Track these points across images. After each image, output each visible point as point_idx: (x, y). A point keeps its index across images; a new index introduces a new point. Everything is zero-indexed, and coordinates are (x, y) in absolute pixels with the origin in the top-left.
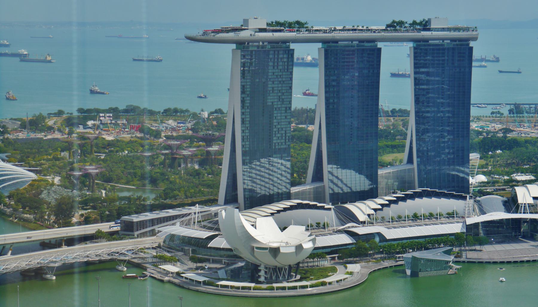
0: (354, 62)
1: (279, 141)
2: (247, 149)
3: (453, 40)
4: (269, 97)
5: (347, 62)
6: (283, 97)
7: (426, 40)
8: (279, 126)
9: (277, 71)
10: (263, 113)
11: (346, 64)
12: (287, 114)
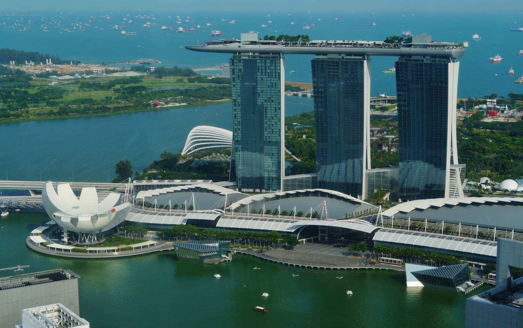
0: (338, 72)
1: (269, 135)
2: (239, 139)
3: (433, 56)
4: (259, 98)
5: (332, 72)
6: (272, 99)
7: (409, 55)
8: (269, 123)
9: (265, 77)
10: (254, 111)
11: (332, 73)
12: (275, 113)
